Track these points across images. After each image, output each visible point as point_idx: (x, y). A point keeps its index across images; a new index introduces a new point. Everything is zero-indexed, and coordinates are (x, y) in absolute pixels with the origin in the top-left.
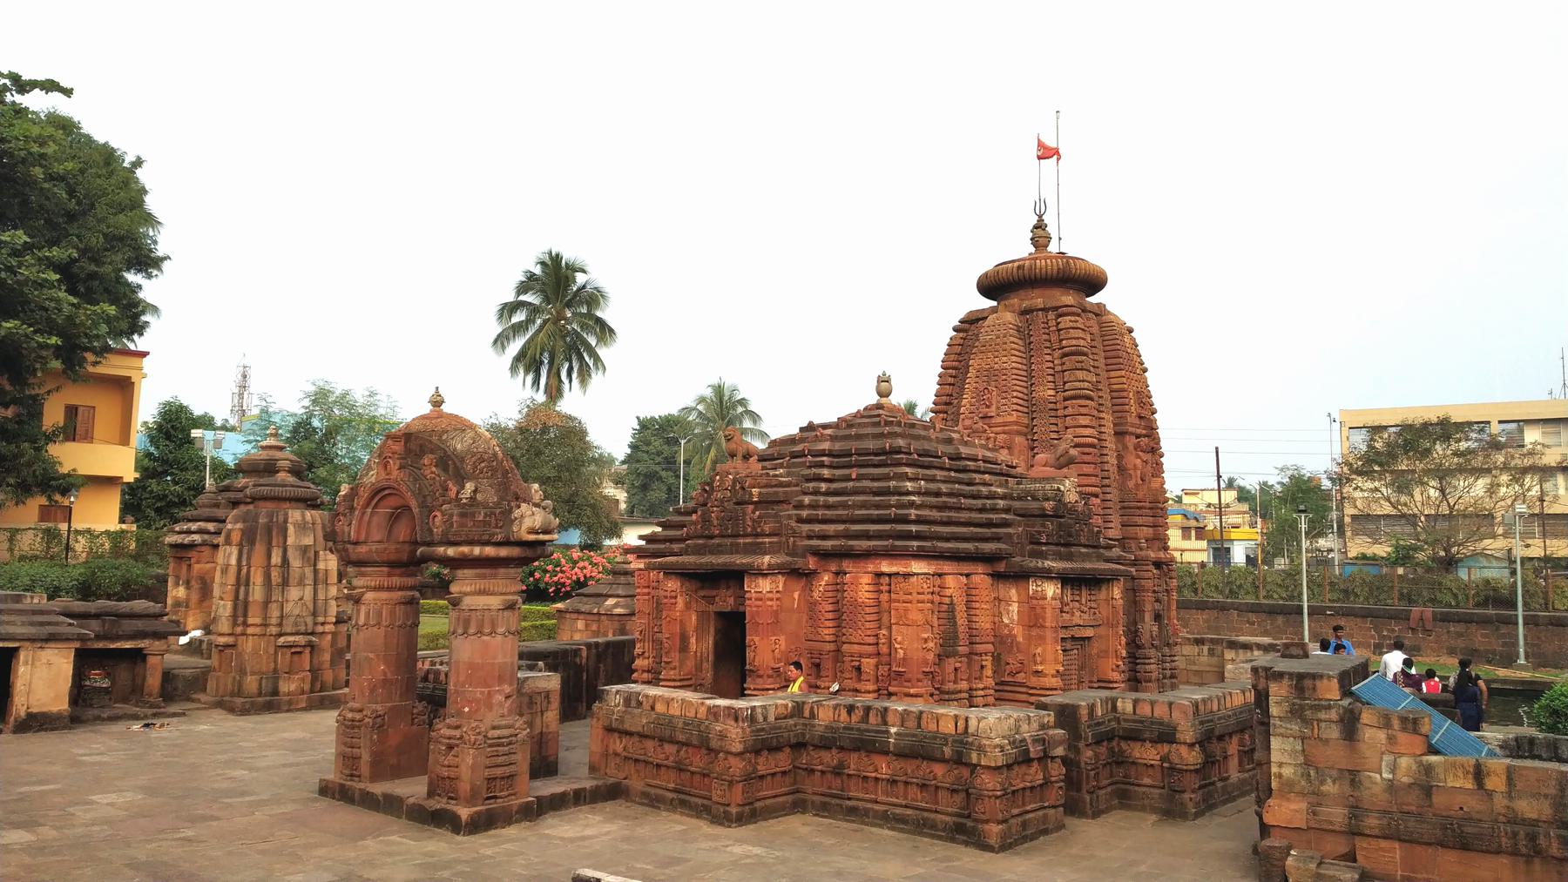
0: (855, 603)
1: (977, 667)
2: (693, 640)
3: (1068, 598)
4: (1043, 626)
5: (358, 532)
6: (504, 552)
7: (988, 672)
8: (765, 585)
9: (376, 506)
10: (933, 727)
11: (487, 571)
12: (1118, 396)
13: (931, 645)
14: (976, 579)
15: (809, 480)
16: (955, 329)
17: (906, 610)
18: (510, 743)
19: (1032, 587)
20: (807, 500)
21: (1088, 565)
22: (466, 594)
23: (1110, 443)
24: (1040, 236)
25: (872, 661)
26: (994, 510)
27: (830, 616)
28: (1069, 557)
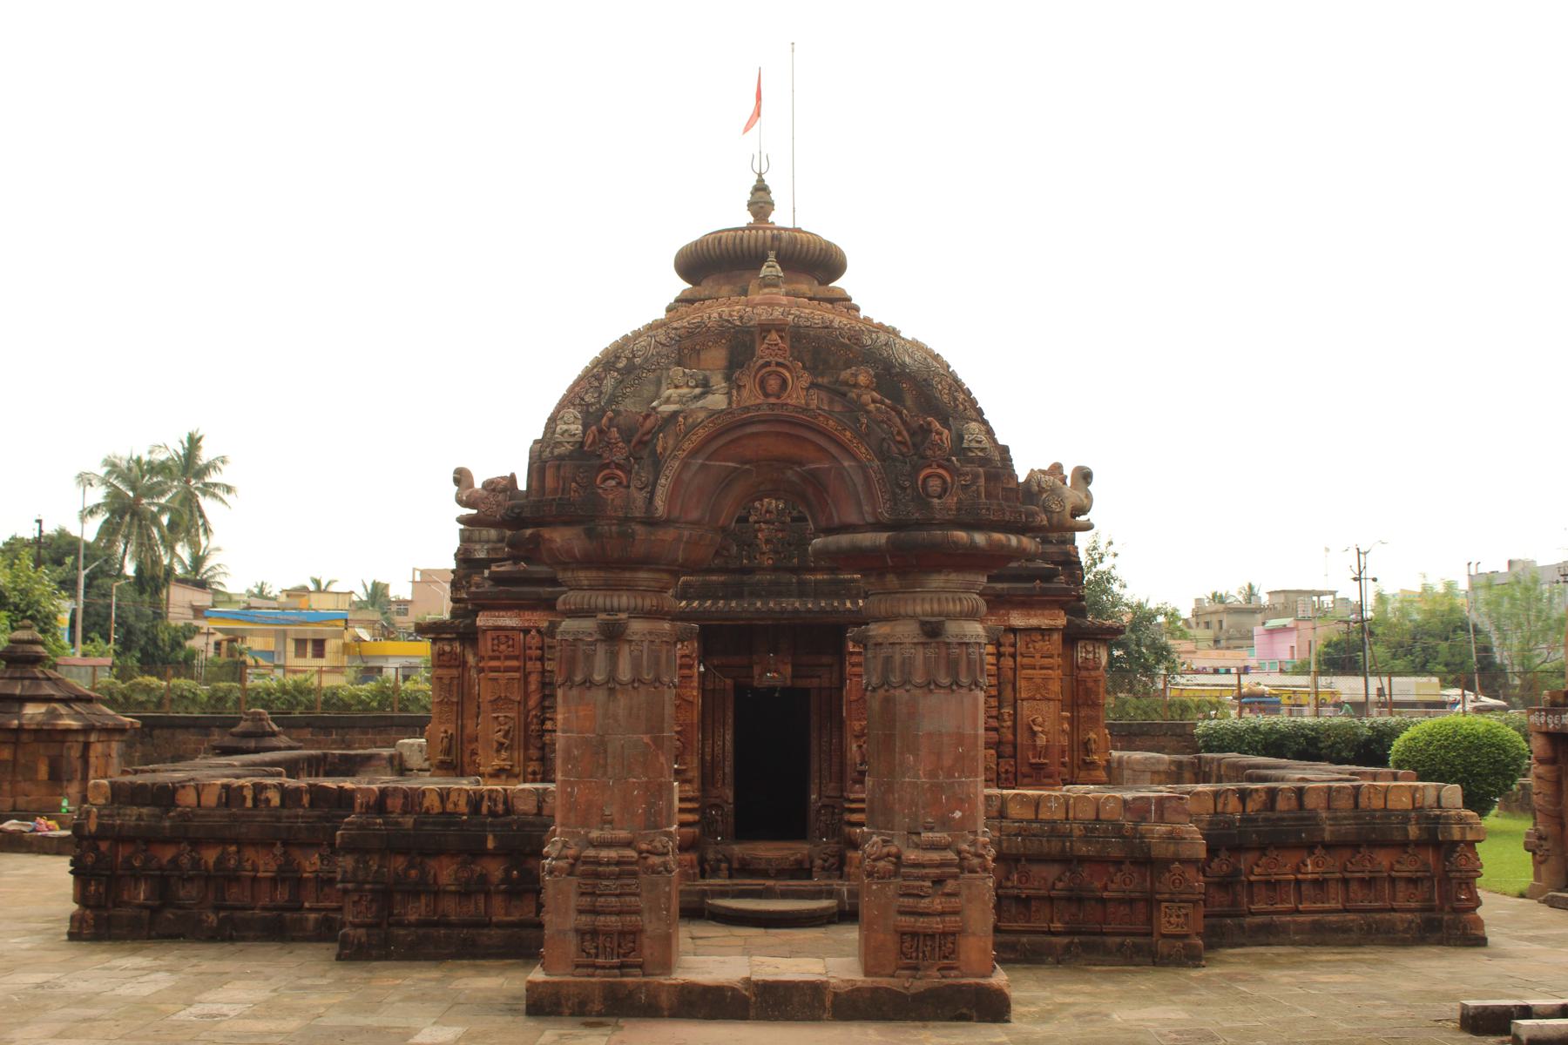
9: (708, 459)
10: (1378, 803)
17: (1046, 679)
19: (1081, 655)
24: (761, 200)
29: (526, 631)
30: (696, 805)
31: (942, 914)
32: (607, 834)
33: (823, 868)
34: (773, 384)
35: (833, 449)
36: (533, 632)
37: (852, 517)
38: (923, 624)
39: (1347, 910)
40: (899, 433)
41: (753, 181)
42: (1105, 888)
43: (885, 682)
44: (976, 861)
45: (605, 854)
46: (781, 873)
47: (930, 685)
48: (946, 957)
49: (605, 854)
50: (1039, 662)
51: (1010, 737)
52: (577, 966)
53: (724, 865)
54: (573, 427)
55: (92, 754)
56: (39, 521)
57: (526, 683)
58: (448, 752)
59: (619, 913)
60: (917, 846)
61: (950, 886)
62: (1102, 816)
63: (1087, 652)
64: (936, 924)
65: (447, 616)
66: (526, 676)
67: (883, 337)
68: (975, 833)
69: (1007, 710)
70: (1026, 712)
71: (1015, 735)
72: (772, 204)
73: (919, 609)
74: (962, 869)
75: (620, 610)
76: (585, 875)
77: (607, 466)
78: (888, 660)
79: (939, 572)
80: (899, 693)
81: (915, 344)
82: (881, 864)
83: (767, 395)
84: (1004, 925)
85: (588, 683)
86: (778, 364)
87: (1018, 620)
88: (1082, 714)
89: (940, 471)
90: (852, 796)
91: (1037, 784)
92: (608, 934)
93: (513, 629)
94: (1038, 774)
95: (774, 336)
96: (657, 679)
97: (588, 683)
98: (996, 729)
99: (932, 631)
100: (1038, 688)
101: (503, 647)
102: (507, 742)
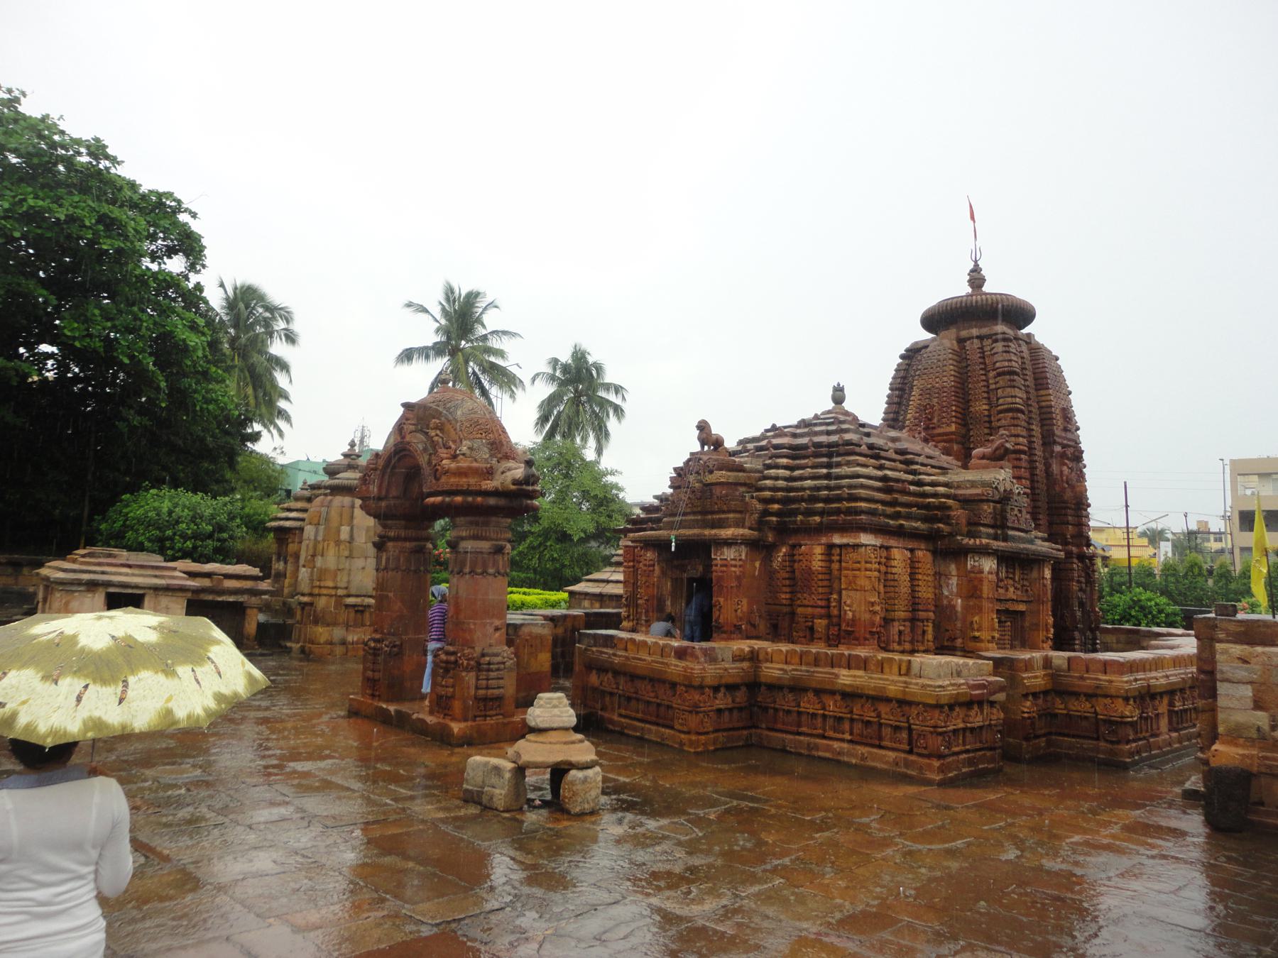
0: (809, 571)
1: (920, 632)
2: (668, 603)
3: (1003, 575)
4: (980, 597)
6: (492, 501)
7: (930, 636)
8: (729, 554)
11: (481, 519)
12: (1046, 416)
13: (877, 608)
14: (920, 554)
15: (769, 467)
16: (902, 357)
17: (855, 577)
18: (498, 670)
19: (970, 563)
20: (768, 482)
21: (1022, 546)
22: (463, 539)
23: (1039, 452)
24: (976, 279)
25: (824, 622)
26: (935, 495)
27: (787, 582)
28: (1006, 538)
41: (971, 265)
87: (837, 539)
91: (849, 645)
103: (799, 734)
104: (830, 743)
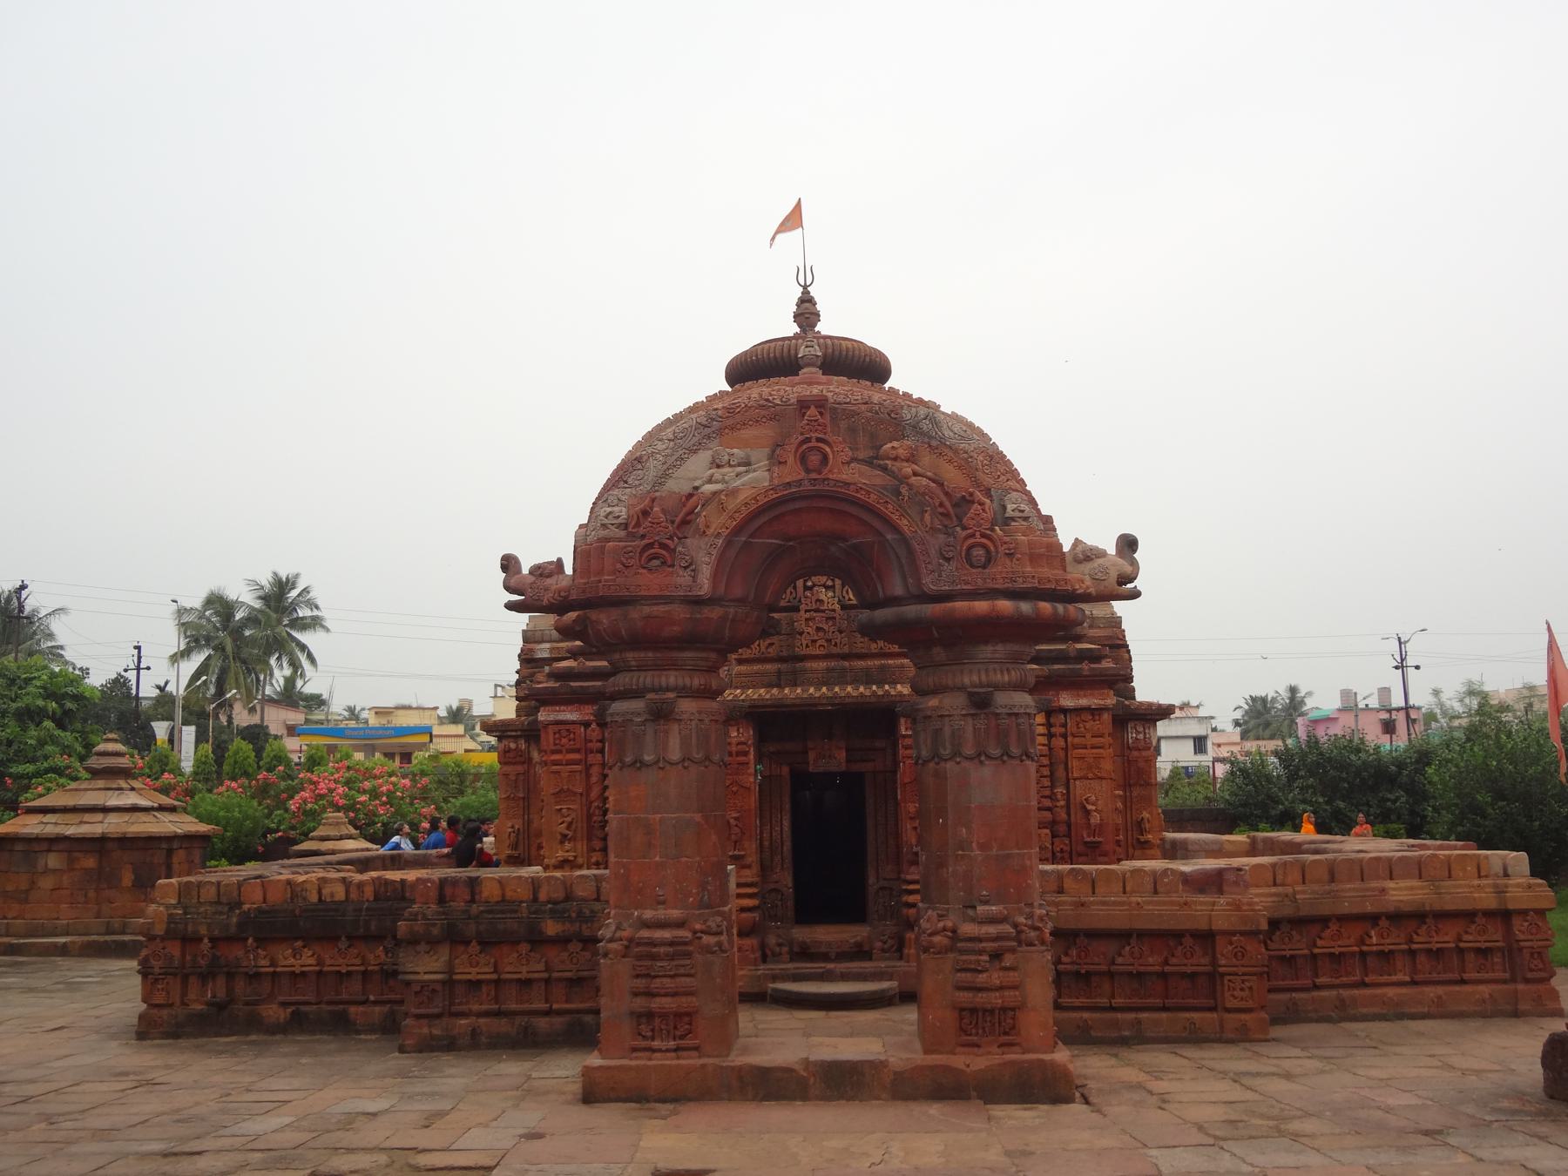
5: (715, 576)
9: (751, 536)
17: (1098, 758)
19: (1131, 735)
24: (806, 312)
29: (587, 724)
30: (755, 890)
31: (1001, 988)
32: (662, 913)
33: (883, 950)
34: (814, 459)
35: (877, 524)
36: (594, 726)
37: (899, 591)
38: (971, 695)
39: (1414, 983)
40: (941, 505)
42: (1166, 963)
43: (936, 756)
44: (1033, 934)
45: (660, 934)
46: (842, 956)
47: (980, 756)
48: (1006, 1033)
49: (660, 934)
50: (1091, 741)
51: (1064, 816)
52: (635, 1050)
53: (785, 949)
54: (616, 509)
55: (175, 860)
56: (138, 648)
57: (588, 776)
58: (515, 846)
59: (675, 994)
60: (973, 920)
61: (1008, 960)
62: (1160, 889)
63: (1138, 733)
64: (995, 999)
65: (513, 715)
66: (588, 768)
67: (922, 412)
68: (1031, 905)
69: (1060, 790)
70: (1078, 792)
71: (1069, 814)
72: (817, 315)
73: (966, 681)
74: (1020, 943)
75: (668, 689)
76: (639, 957)
77: (650, 546)
78: (938, 732)
79: (986, 642)
80: (949, 765)
81: (955, 417)
82: (937, 939)
83: (808, 471)
84: (1064, 1001)
85: (639, 764)
86: (818, 440)
87: (1067, 700)
88: (1135, 794)
89: (984, 540)
90: (909, 877)
92: (664, 1016)
93: (573, 723)
94: (1093, 852)
95: (812, 411)
96: (707, 758)
97: (639, 764)
98: (1049, 809)
99: (980, 702)
100: (1090, 768)
101: (564, 741)
102: (570, 834)
103: (1316, 987)
104: (1379, 991)
